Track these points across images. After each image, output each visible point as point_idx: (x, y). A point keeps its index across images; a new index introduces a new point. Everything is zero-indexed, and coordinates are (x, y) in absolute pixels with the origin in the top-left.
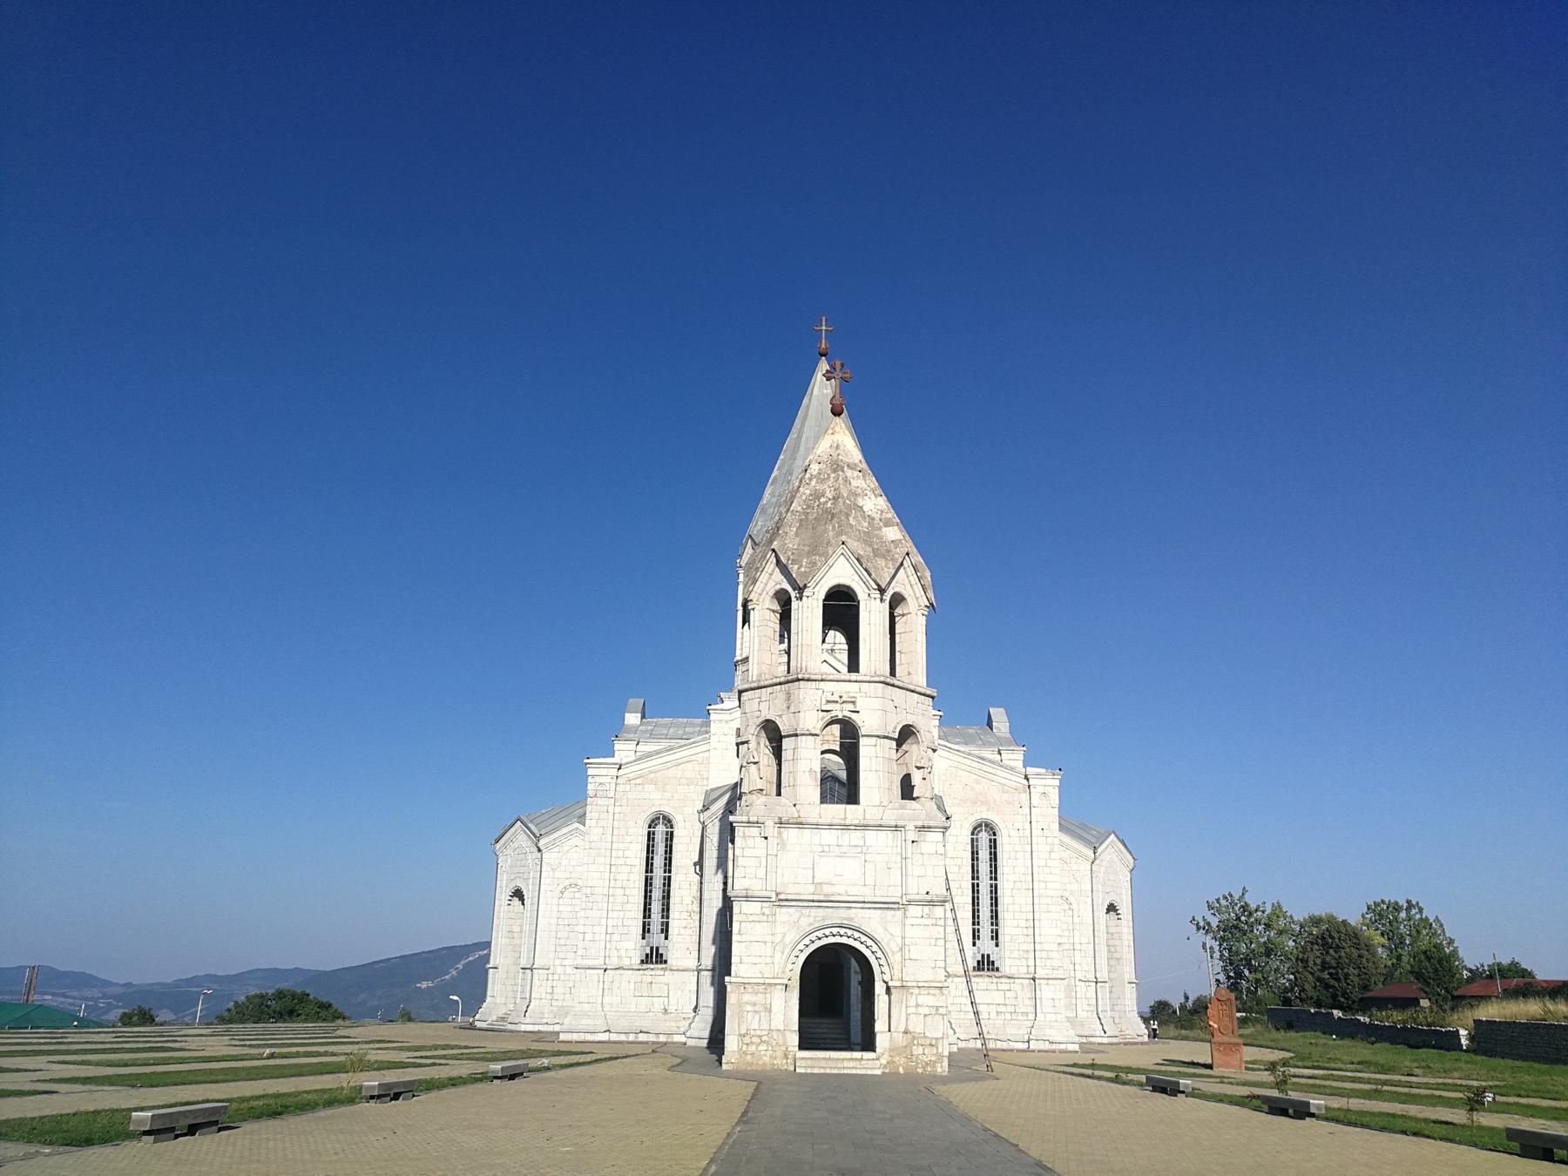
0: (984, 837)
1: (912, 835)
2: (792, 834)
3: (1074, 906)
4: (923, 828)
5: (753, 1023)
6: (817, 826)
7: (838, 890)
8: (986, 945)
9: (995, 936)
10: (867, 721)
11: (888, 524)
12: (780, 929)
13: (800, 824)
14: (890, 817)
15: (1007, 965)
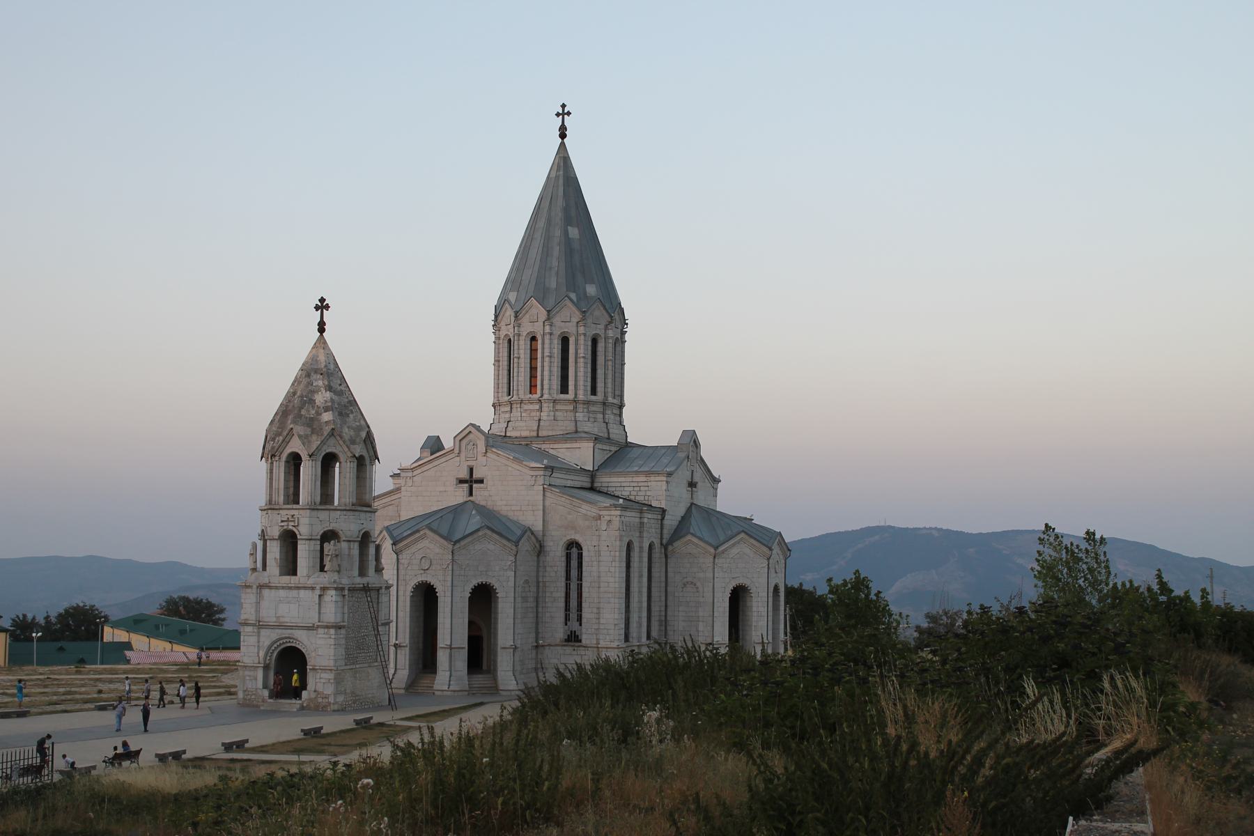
0: (574, 550)
1: (318, 592)
2: (266, 592)
3: (701, 589)
4: (324, 589)
5: (249, 685)
6: (276, 588)
7: (287, 620)
8: (574, 625)
9: (580, 619)
10: (303, 530)
11: (326, 409)
12: (262, 639)
13: (270, 587)
14: (310, 582)
15: (586, 639)
